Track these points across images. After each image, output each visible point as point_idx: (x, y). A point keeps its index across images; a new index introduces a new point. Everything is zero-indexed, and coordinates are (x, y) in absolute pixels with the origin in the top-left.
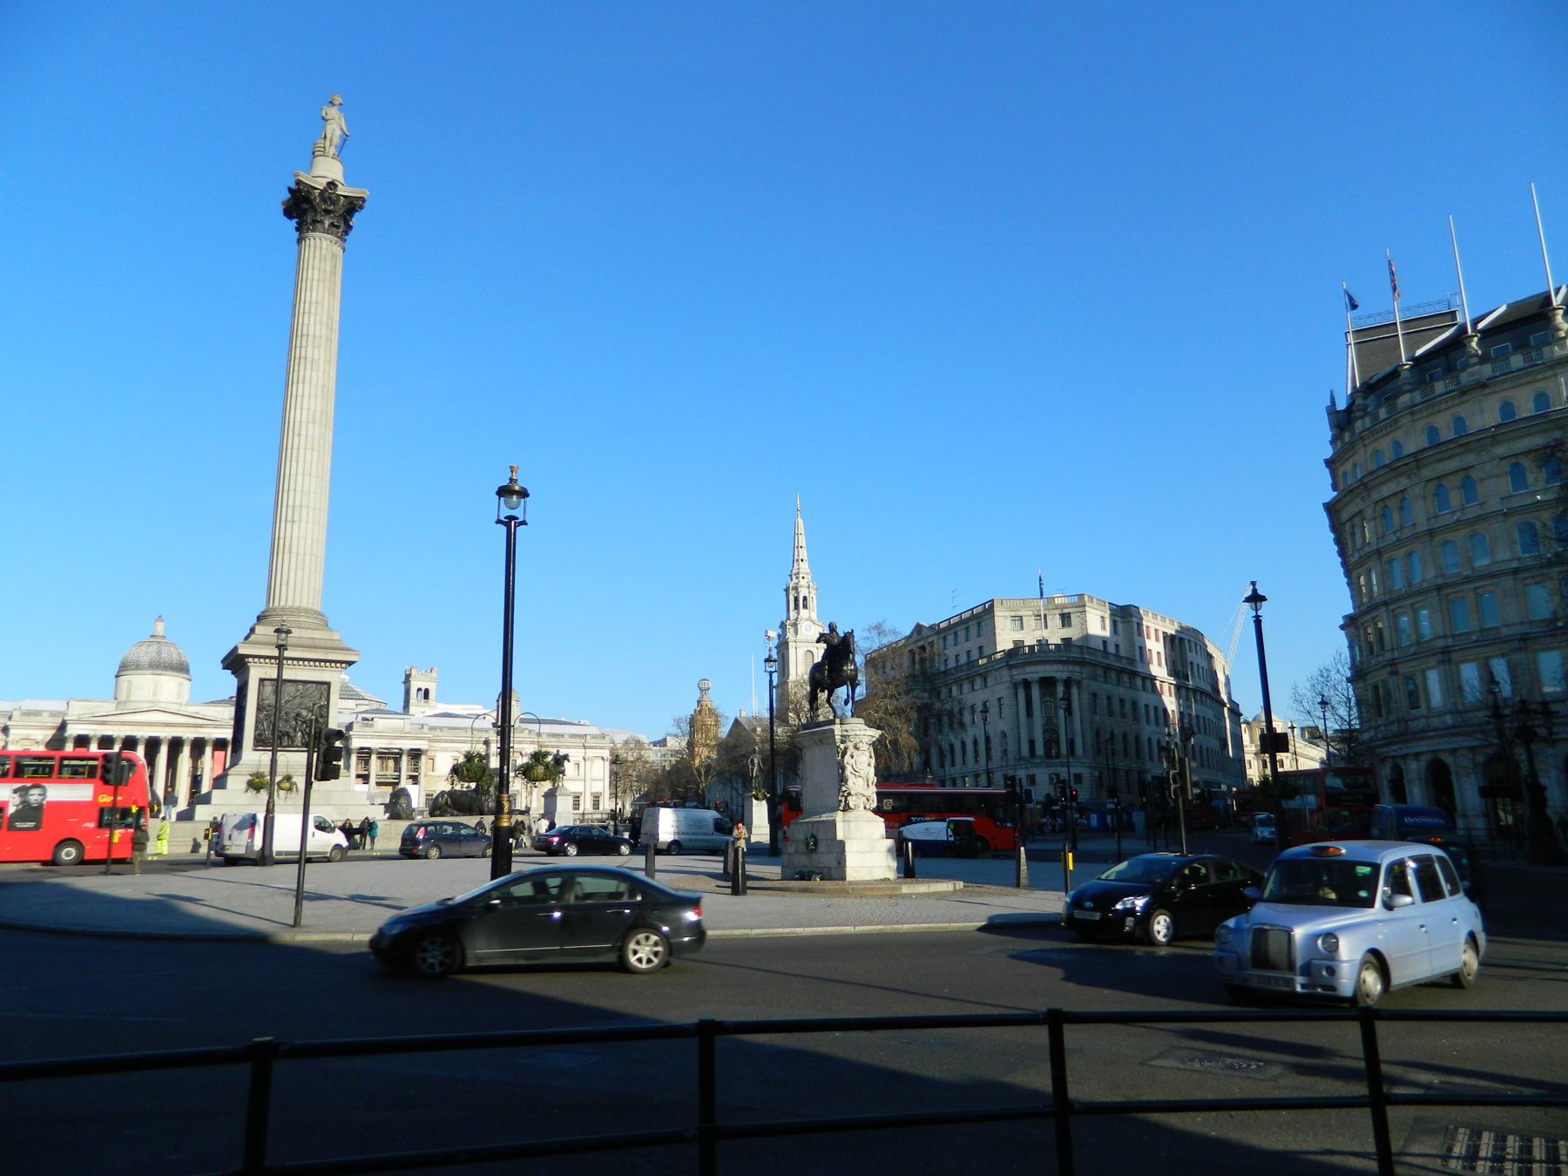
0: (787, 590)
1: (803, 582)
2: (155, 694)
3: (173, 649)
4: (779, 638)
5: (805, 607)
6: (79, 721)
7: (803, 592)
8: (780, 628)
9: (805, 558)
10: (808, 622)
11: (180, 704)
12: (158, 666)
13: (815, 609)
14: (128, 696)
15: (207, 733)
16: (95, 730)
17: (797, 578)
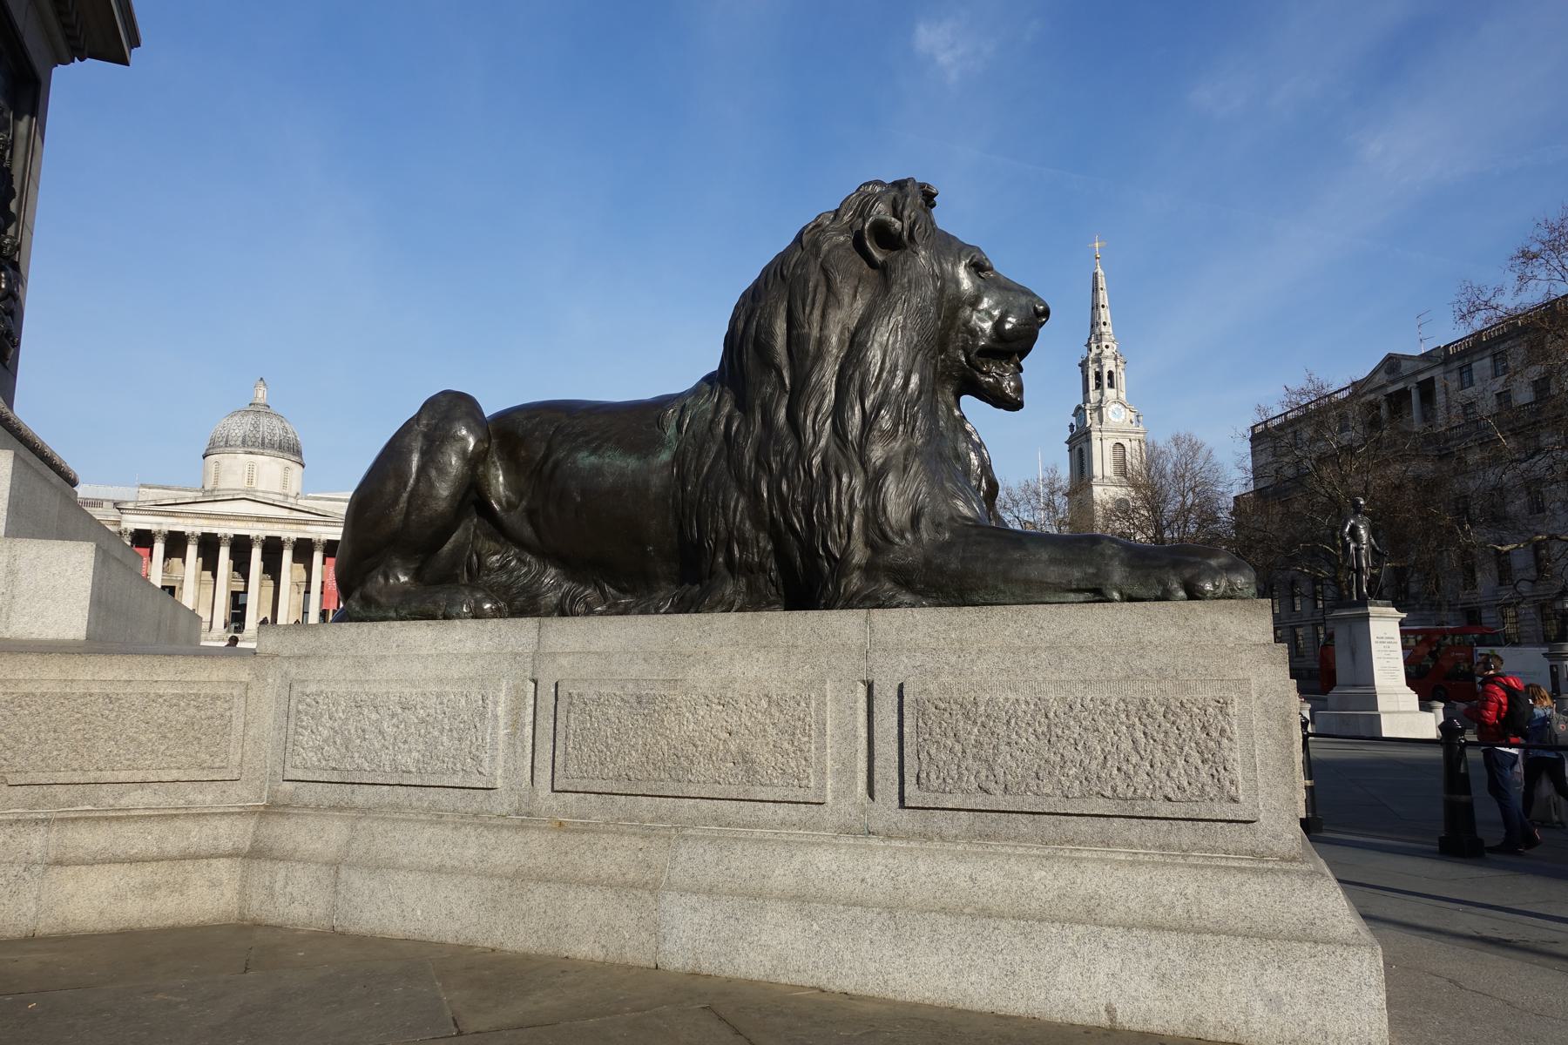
0: (1084, 365)
1: (1107, 352)
2: (250, 481)
3: (275, 421)
4: (1072, 430)
5: (1111, 385)
6: (137, 511)
7: (1109, 365)
8: (1074, 415)
9: (1109, 321)
10: (1117, 405)
11: (287, 496)
12: (256, 444)
13: (1124, 389)
14: (216, 483)
15: (316, 533)
16: (161, 524)
17: (1098, 347)
